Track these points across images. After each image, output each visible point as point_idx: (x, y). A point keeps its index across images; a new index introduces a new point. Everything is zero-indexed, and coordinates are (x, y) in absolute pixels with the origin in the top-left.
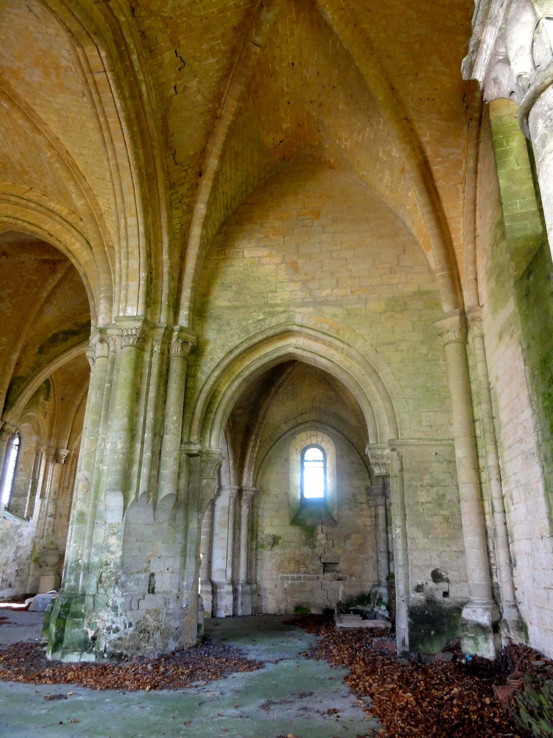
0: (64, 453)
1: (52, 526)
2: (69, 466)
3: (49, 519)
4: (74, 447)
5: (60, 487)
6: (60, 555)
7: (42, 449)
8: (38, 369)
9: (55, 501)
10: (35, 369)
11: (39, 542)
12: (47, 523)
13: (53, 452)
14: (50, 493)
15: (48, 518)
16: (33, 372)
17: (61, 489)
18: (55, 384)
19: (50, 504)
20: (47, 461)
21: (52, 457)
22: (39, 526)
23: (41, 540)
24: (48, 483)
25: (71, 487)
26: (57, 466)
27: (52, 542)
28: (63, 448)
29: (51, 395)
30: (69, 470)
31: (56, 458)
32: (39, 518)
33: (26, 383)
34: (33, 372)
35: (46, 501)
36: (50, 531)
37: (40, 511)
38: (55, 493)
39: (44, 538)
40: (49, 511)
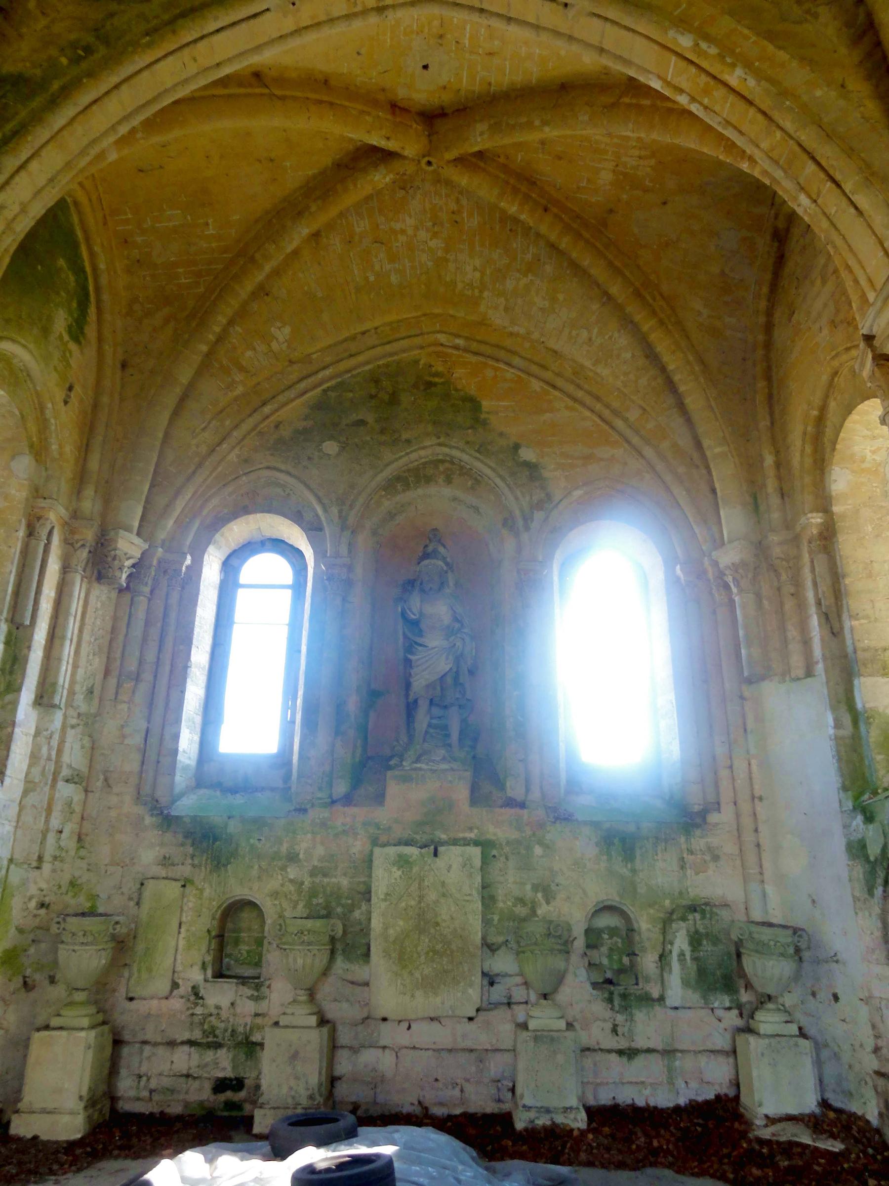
0: (129, 546)
1: (76, 817)
2: (142, 603)
3: (65, 791)
4: (162, 535)
5: (107, 673)
6: (114, 937)
7: (52, 516)
8: (102, 51)
9: (90, 724)
10: (89, 50)
11: (24, 883)
12: (57, 808)
13: (89, 535)
14: (72, 693)
15: (61, 784)
16: (76, 61)
17: (112, 681)
18: (105, 297)
19: (71, 733)
20: (66, 569)
21: (84, 554)
22: (28, 818)
23: (37, 873)
24: (67, 651)
25: (147, 676)
26: (101, 594)
27: (72, 884)
28: (128, 529)
29: (91, 331)
30: (140, 614)
31: (100, 563)
32: (29, 786)
33: (36, 103)
34: (76, 61)
35: (58, 716)
36: (68, 841)
37: (34, 757)
38: (91, 691)
39: (47, 867)
40: (66, 759)
